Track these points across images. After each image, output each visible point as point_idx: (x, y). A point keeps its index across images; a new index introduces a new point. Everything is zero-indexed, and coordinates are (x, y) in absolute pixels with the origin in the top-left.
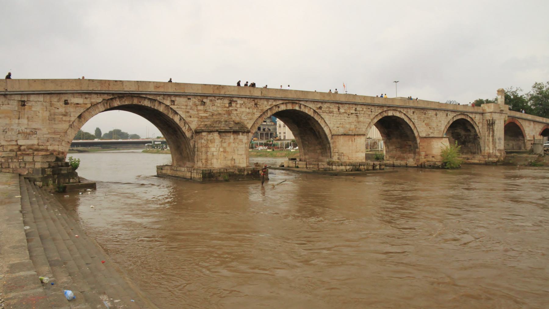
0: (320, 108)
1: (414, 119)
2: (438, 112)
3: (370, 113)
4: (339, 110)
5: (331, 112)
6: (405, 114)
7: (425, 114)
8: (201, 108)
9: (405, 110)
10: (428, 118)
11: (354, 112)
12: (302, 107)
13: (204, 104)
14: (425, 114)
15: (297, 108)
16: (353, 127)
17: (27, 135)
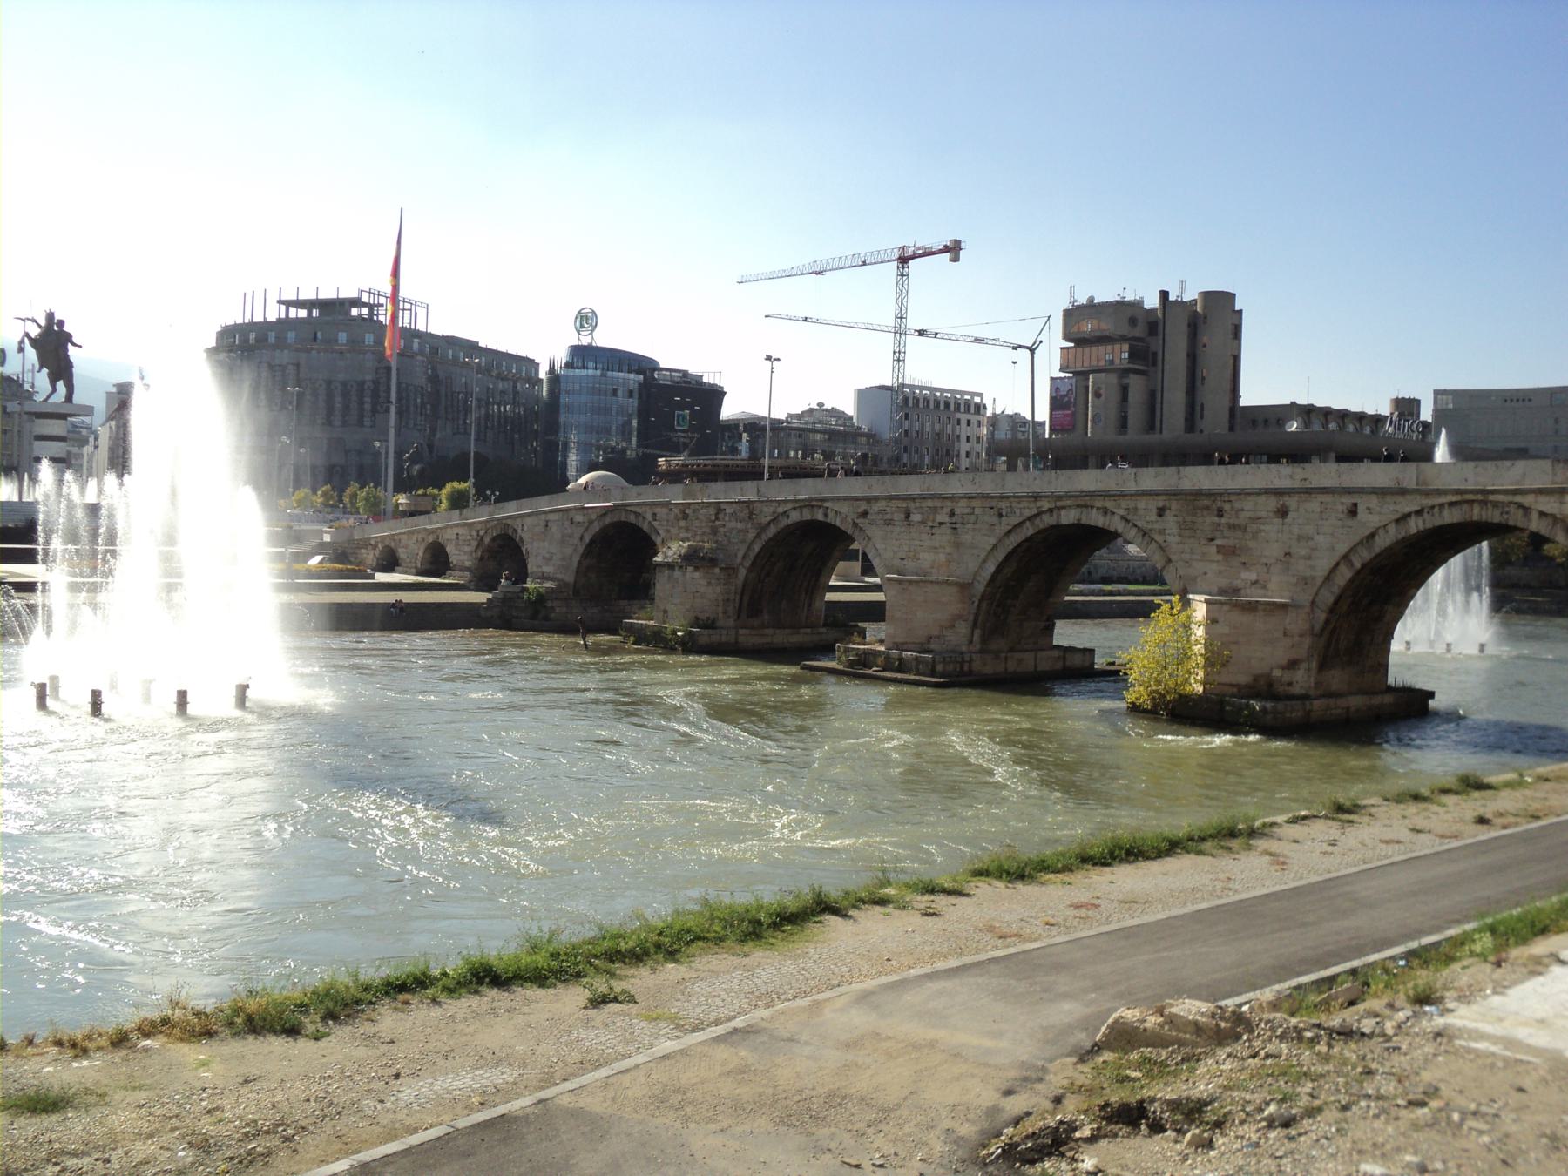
0: (865, 514)
1: (1162, 532)
2: (1292, 502)
3: (995, 520)
4: (908, 516)
5: (889, 523)
6: (1123, 518)
7: (1220, 513)
8: (682, 523)
9: (1124, 503)
10: (1233, 527)
11: (946, 519)
12: (831, 514)
13: (685, 517)
14: (1220, 513)
15: (820, 517)
16: (942, 558)
17: (548, 560)
